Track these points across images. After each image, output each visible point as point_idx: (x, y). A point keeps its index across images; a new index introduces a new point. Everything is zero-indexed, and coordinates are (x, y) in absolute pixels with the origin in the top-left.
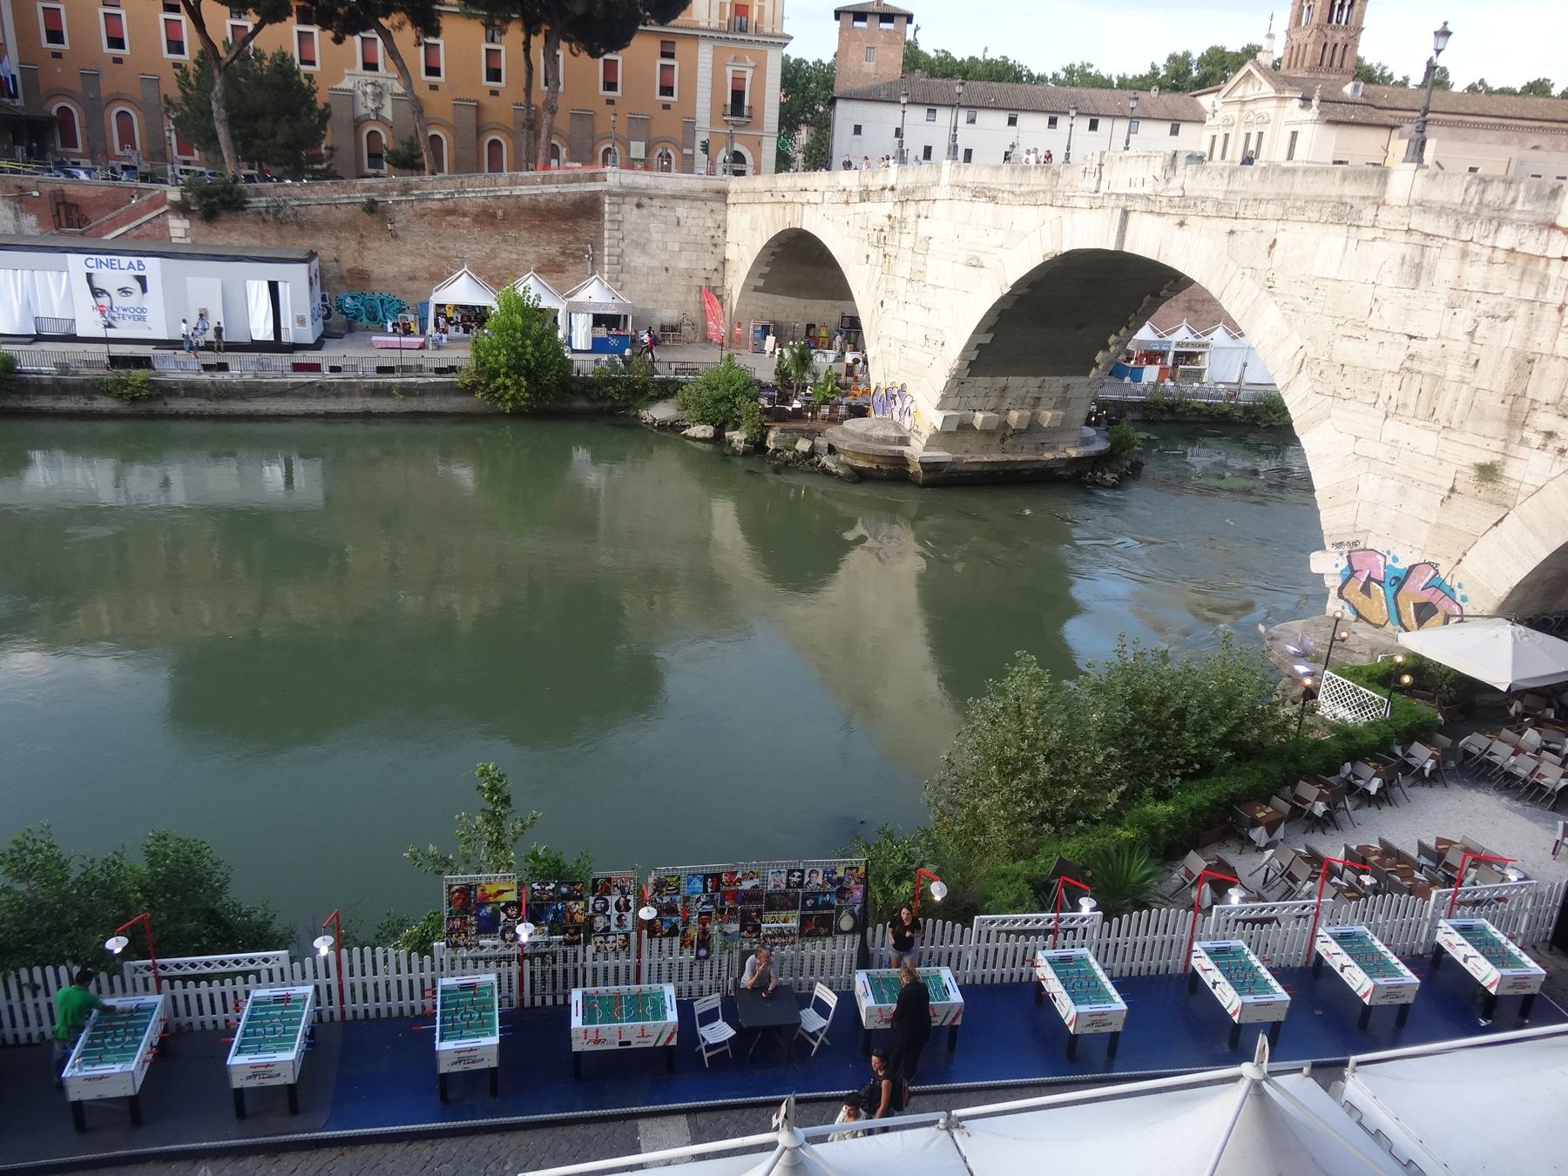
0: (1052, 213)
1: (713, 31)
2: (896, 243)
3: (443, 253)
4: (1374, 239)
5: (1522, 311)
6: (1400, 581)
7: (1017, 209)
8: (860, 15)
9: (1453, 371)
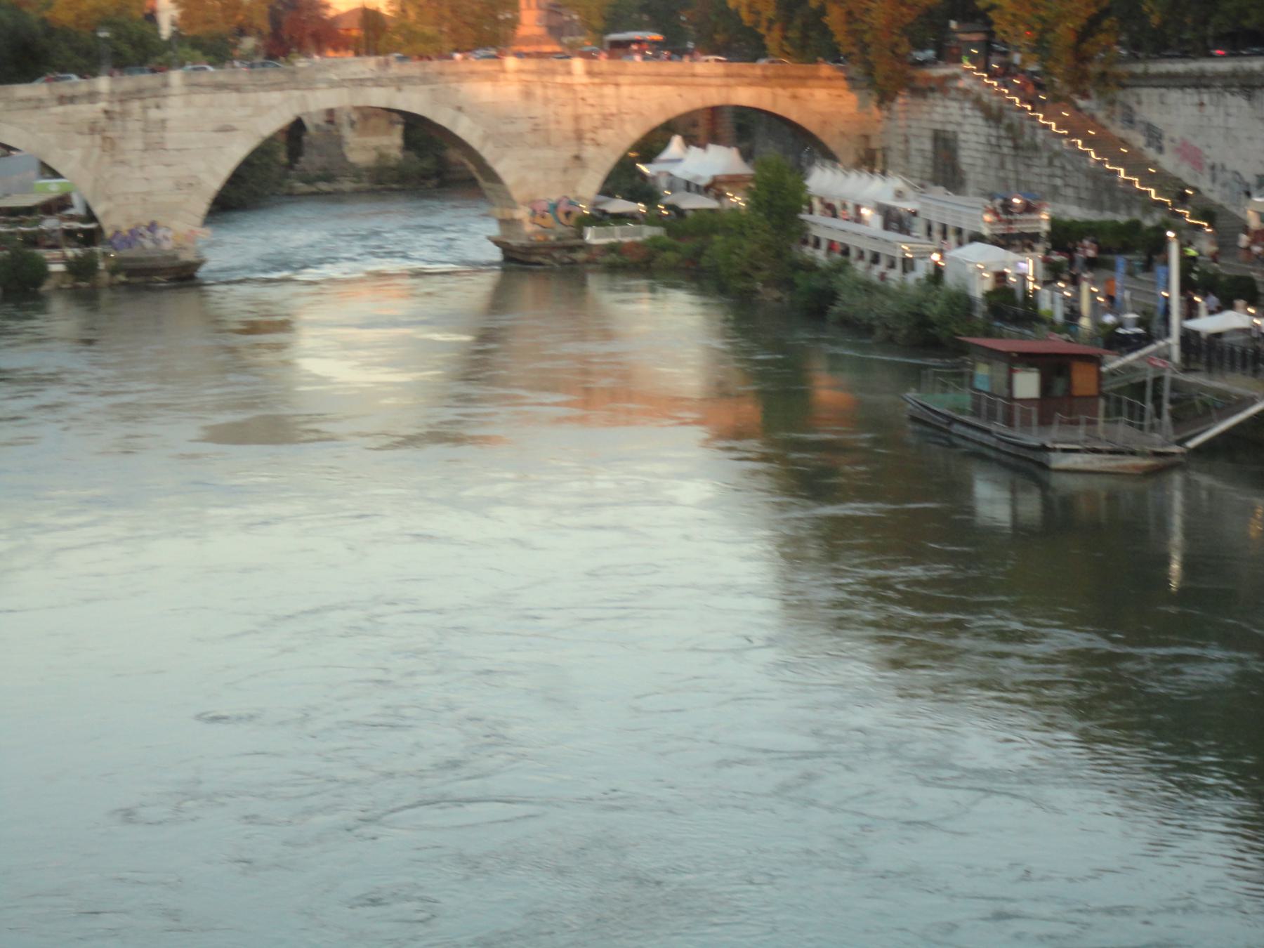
0: (296, 93)
6: (555, 207)
9: (553, 126)
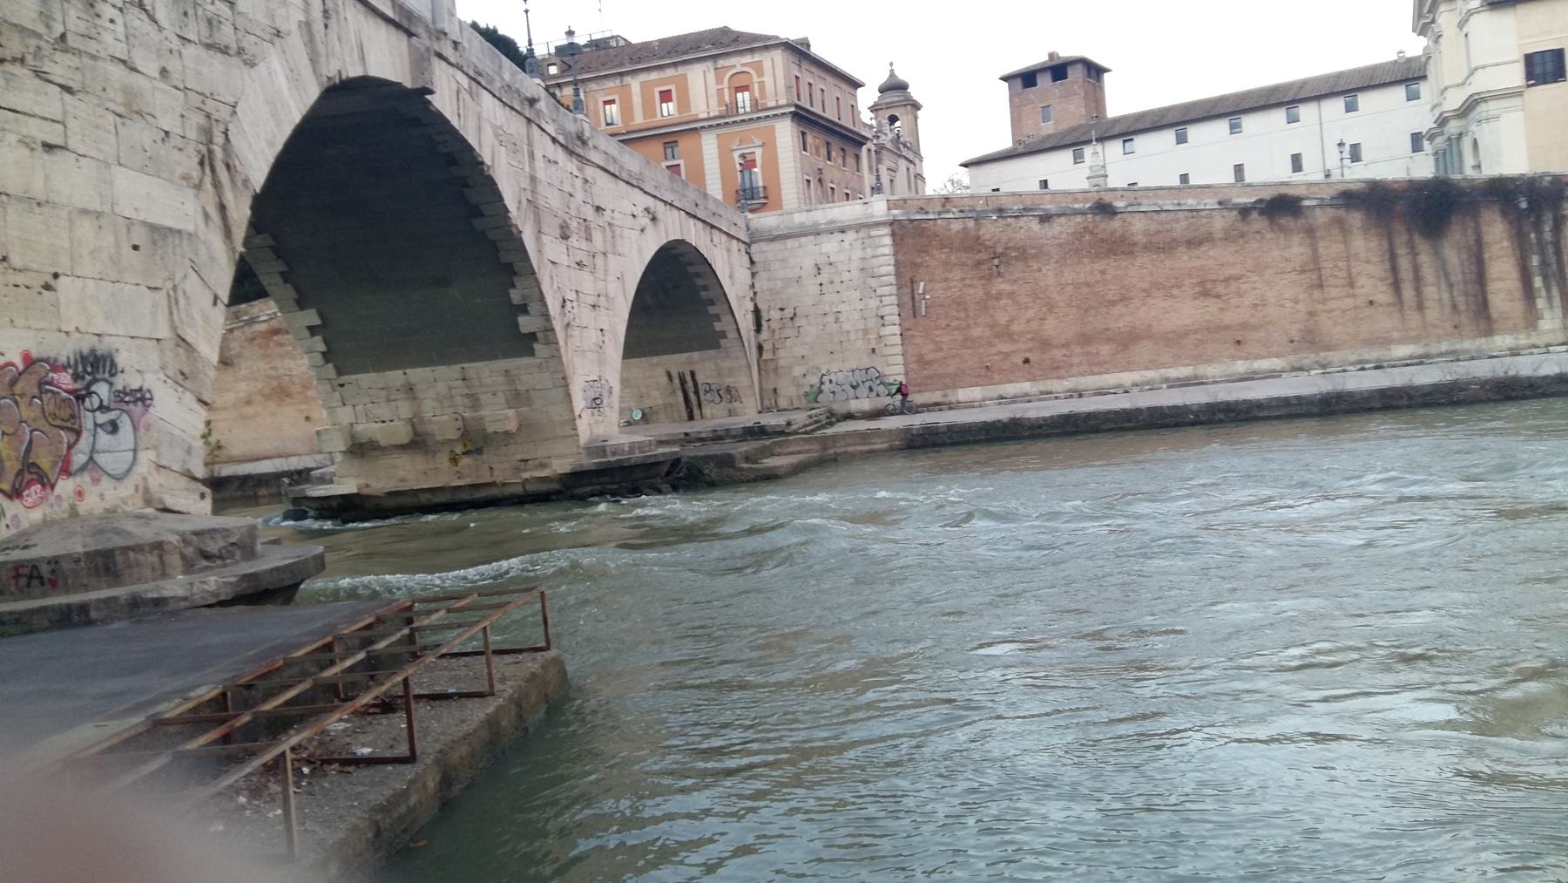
1: (715, 118)
3: (273, 373)
8: (1027, 78)
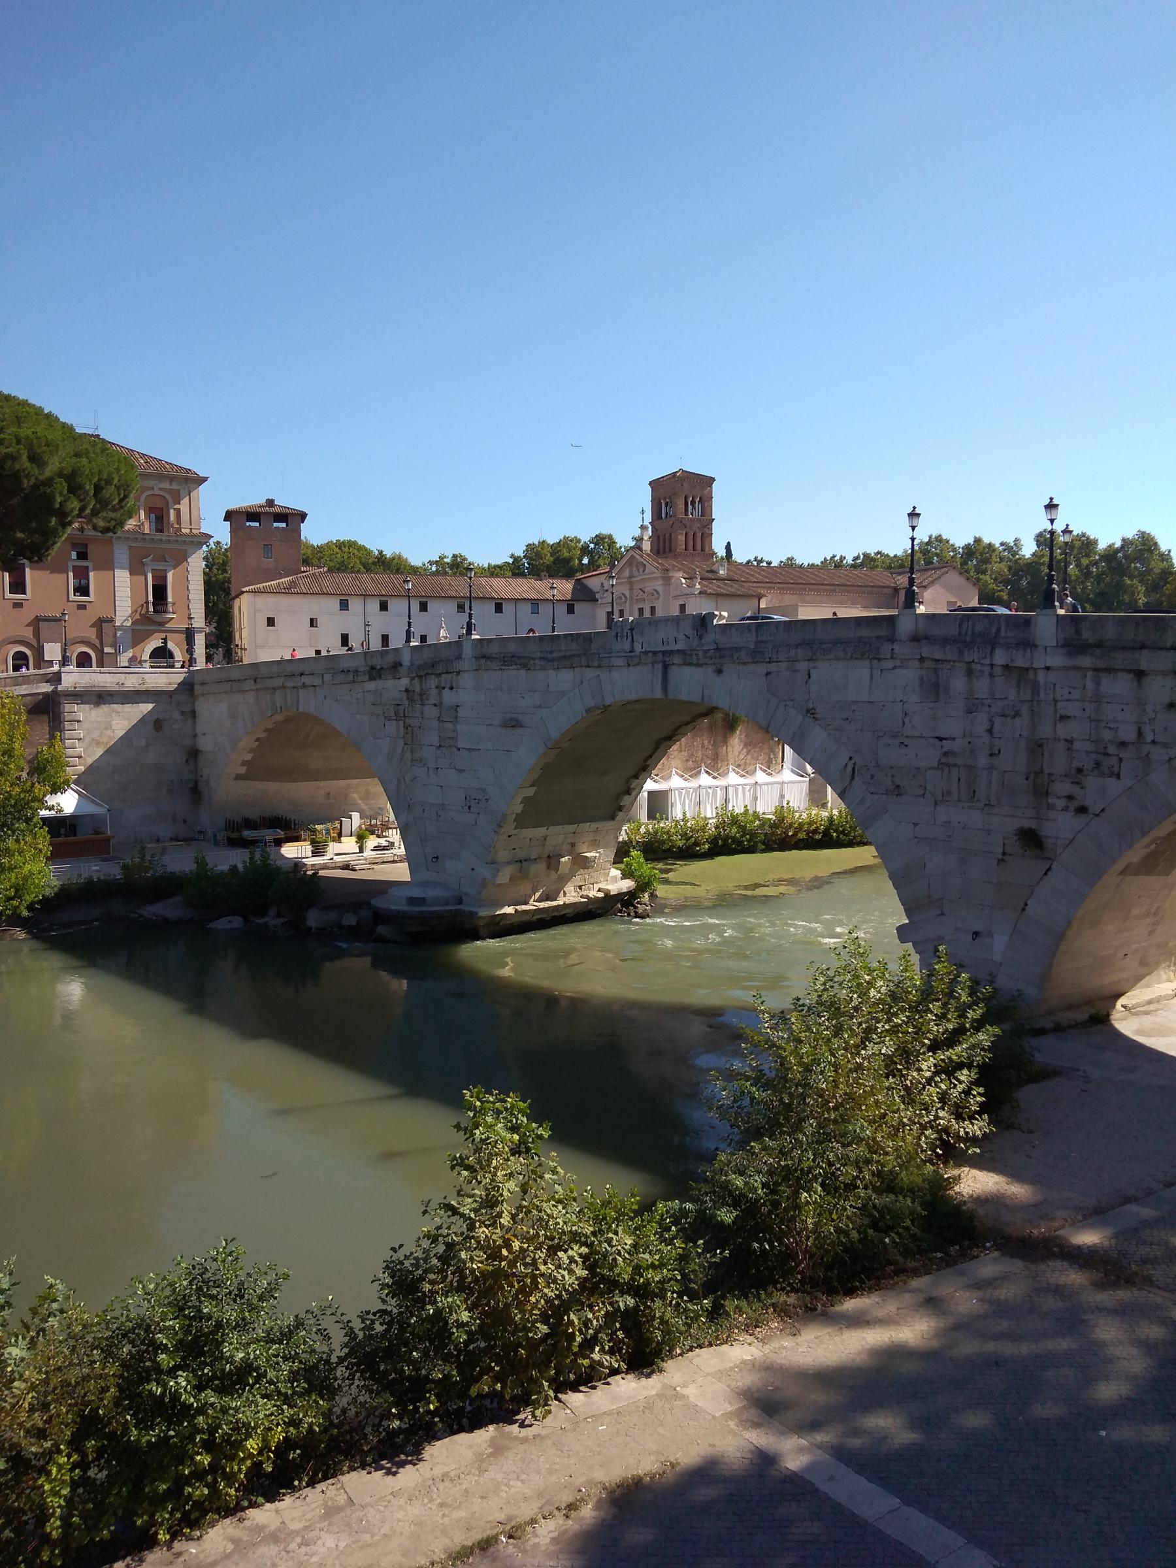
0: (590, 673)
2: (419, 715)
4: (894, 668)
5: (1025, 709)
7: (551, 673)
